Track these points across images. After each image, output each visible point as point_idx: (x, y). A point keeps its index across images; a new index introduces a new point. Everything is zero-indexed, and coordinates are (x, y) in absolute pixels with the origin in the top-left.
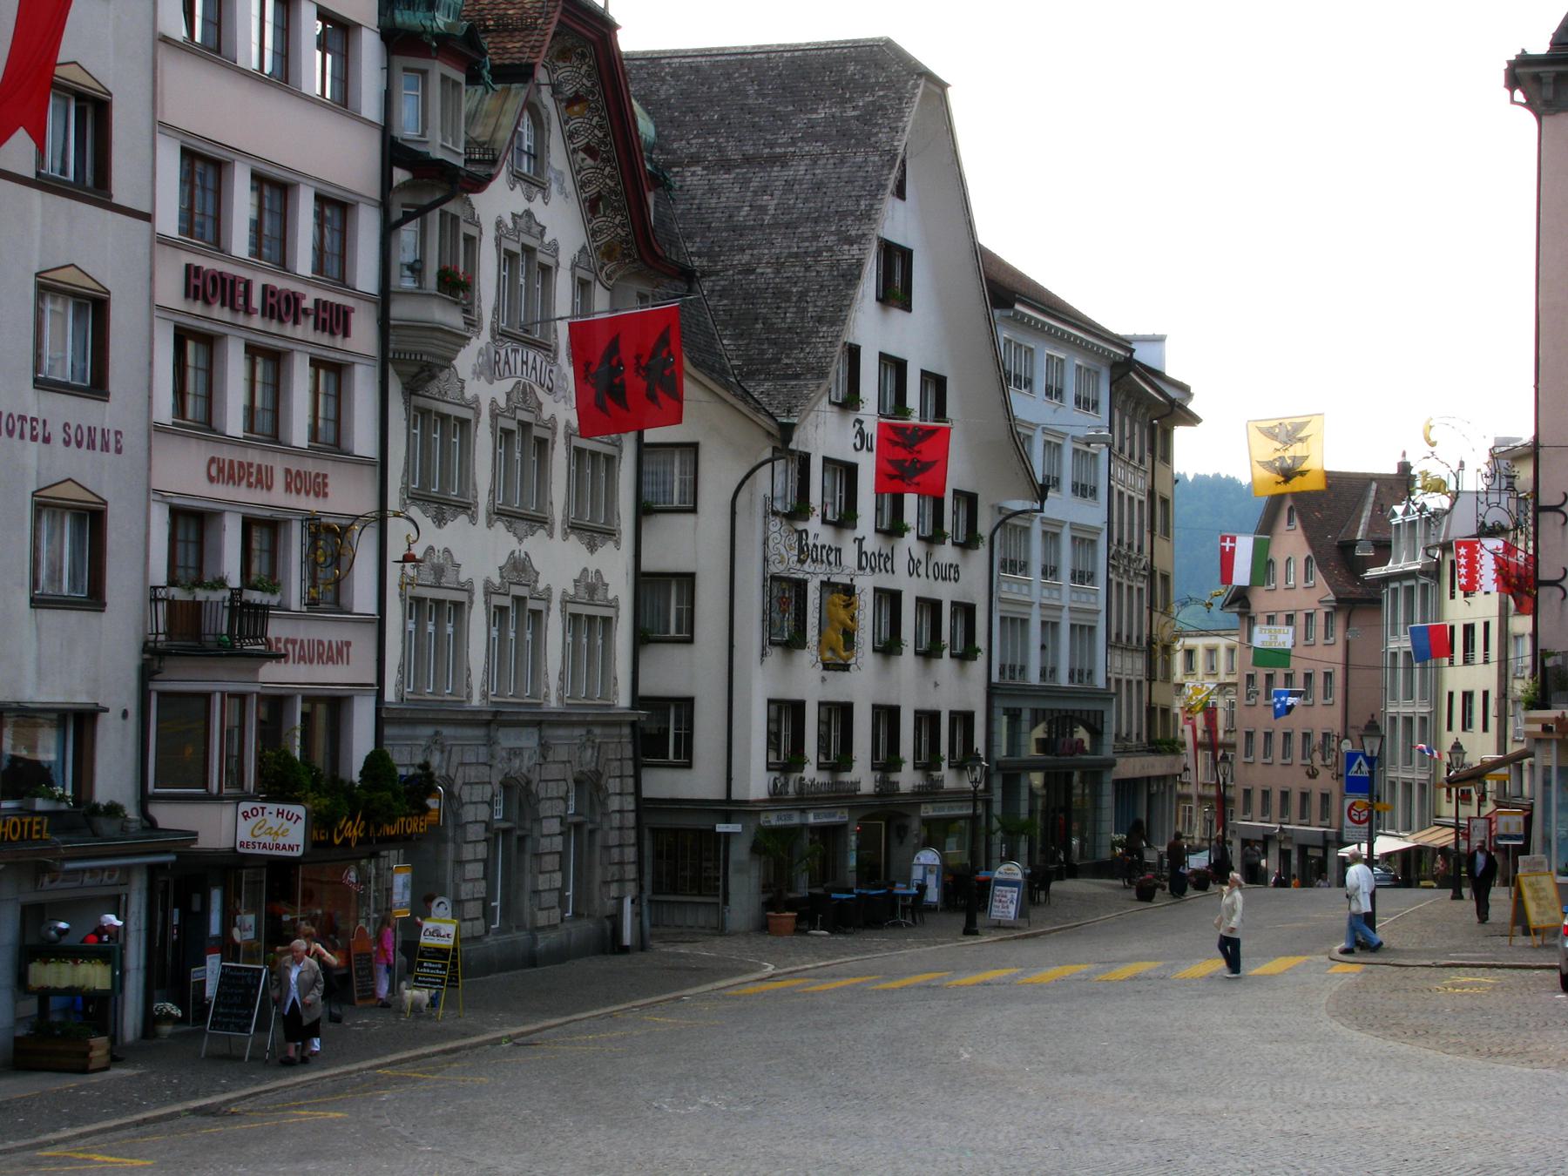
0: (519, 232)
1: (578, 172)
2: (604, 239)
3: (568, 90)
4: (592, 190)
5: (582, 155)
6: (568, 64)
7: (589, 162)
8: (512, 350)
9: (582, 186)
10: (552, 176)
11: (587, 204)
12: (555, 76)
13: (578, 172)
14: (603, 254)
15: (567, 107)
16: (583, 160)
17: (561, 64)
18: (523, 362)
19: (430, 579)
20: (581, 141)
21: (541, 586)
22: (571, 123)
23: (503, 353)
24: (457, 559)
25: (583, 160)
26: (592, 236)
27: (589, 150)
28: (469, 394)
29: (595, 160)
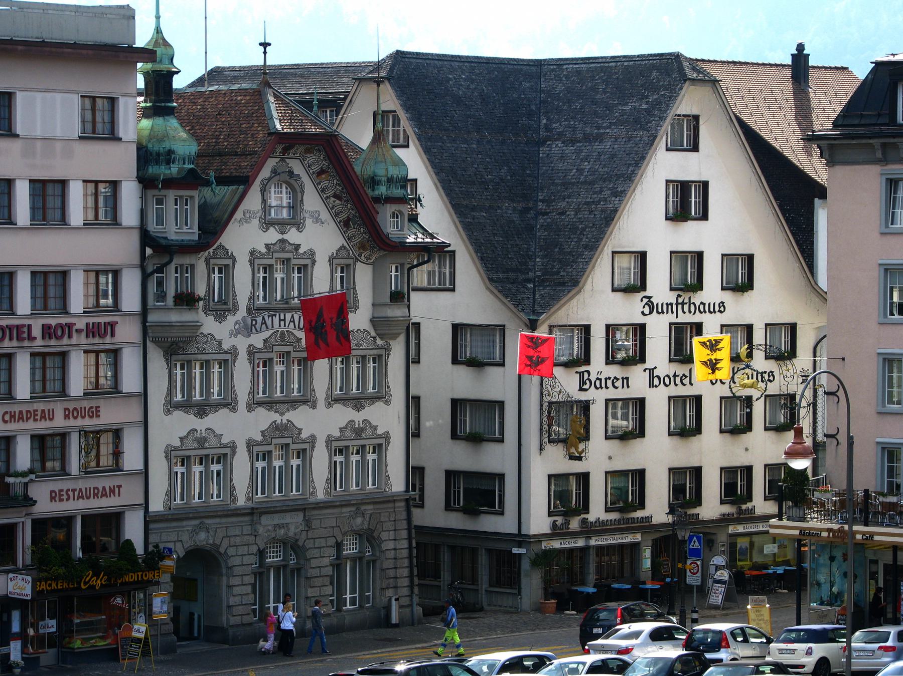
0: (272, 252)
1: (332, 208)
2: (357, 240)
3: (316, 168)
4: (344, 216)
5: (333, 199)
7: (338, 202)
8: (269, 316)
10: (307, 215)
12: (306, 162)
13: (332, 208)
14: (359, 248)
15: (317, 177)
16: (334, 202)
17: (308, 155)
18: (280, 320)
19: (195, 445)
20: (330, 193)
21: (304, 435)
23: (259, 320)
24: (218, 432)
25: (334, 202)
26: (349, 239)
27: (335, 196)
28: (225, 346)
29: (341, 201)
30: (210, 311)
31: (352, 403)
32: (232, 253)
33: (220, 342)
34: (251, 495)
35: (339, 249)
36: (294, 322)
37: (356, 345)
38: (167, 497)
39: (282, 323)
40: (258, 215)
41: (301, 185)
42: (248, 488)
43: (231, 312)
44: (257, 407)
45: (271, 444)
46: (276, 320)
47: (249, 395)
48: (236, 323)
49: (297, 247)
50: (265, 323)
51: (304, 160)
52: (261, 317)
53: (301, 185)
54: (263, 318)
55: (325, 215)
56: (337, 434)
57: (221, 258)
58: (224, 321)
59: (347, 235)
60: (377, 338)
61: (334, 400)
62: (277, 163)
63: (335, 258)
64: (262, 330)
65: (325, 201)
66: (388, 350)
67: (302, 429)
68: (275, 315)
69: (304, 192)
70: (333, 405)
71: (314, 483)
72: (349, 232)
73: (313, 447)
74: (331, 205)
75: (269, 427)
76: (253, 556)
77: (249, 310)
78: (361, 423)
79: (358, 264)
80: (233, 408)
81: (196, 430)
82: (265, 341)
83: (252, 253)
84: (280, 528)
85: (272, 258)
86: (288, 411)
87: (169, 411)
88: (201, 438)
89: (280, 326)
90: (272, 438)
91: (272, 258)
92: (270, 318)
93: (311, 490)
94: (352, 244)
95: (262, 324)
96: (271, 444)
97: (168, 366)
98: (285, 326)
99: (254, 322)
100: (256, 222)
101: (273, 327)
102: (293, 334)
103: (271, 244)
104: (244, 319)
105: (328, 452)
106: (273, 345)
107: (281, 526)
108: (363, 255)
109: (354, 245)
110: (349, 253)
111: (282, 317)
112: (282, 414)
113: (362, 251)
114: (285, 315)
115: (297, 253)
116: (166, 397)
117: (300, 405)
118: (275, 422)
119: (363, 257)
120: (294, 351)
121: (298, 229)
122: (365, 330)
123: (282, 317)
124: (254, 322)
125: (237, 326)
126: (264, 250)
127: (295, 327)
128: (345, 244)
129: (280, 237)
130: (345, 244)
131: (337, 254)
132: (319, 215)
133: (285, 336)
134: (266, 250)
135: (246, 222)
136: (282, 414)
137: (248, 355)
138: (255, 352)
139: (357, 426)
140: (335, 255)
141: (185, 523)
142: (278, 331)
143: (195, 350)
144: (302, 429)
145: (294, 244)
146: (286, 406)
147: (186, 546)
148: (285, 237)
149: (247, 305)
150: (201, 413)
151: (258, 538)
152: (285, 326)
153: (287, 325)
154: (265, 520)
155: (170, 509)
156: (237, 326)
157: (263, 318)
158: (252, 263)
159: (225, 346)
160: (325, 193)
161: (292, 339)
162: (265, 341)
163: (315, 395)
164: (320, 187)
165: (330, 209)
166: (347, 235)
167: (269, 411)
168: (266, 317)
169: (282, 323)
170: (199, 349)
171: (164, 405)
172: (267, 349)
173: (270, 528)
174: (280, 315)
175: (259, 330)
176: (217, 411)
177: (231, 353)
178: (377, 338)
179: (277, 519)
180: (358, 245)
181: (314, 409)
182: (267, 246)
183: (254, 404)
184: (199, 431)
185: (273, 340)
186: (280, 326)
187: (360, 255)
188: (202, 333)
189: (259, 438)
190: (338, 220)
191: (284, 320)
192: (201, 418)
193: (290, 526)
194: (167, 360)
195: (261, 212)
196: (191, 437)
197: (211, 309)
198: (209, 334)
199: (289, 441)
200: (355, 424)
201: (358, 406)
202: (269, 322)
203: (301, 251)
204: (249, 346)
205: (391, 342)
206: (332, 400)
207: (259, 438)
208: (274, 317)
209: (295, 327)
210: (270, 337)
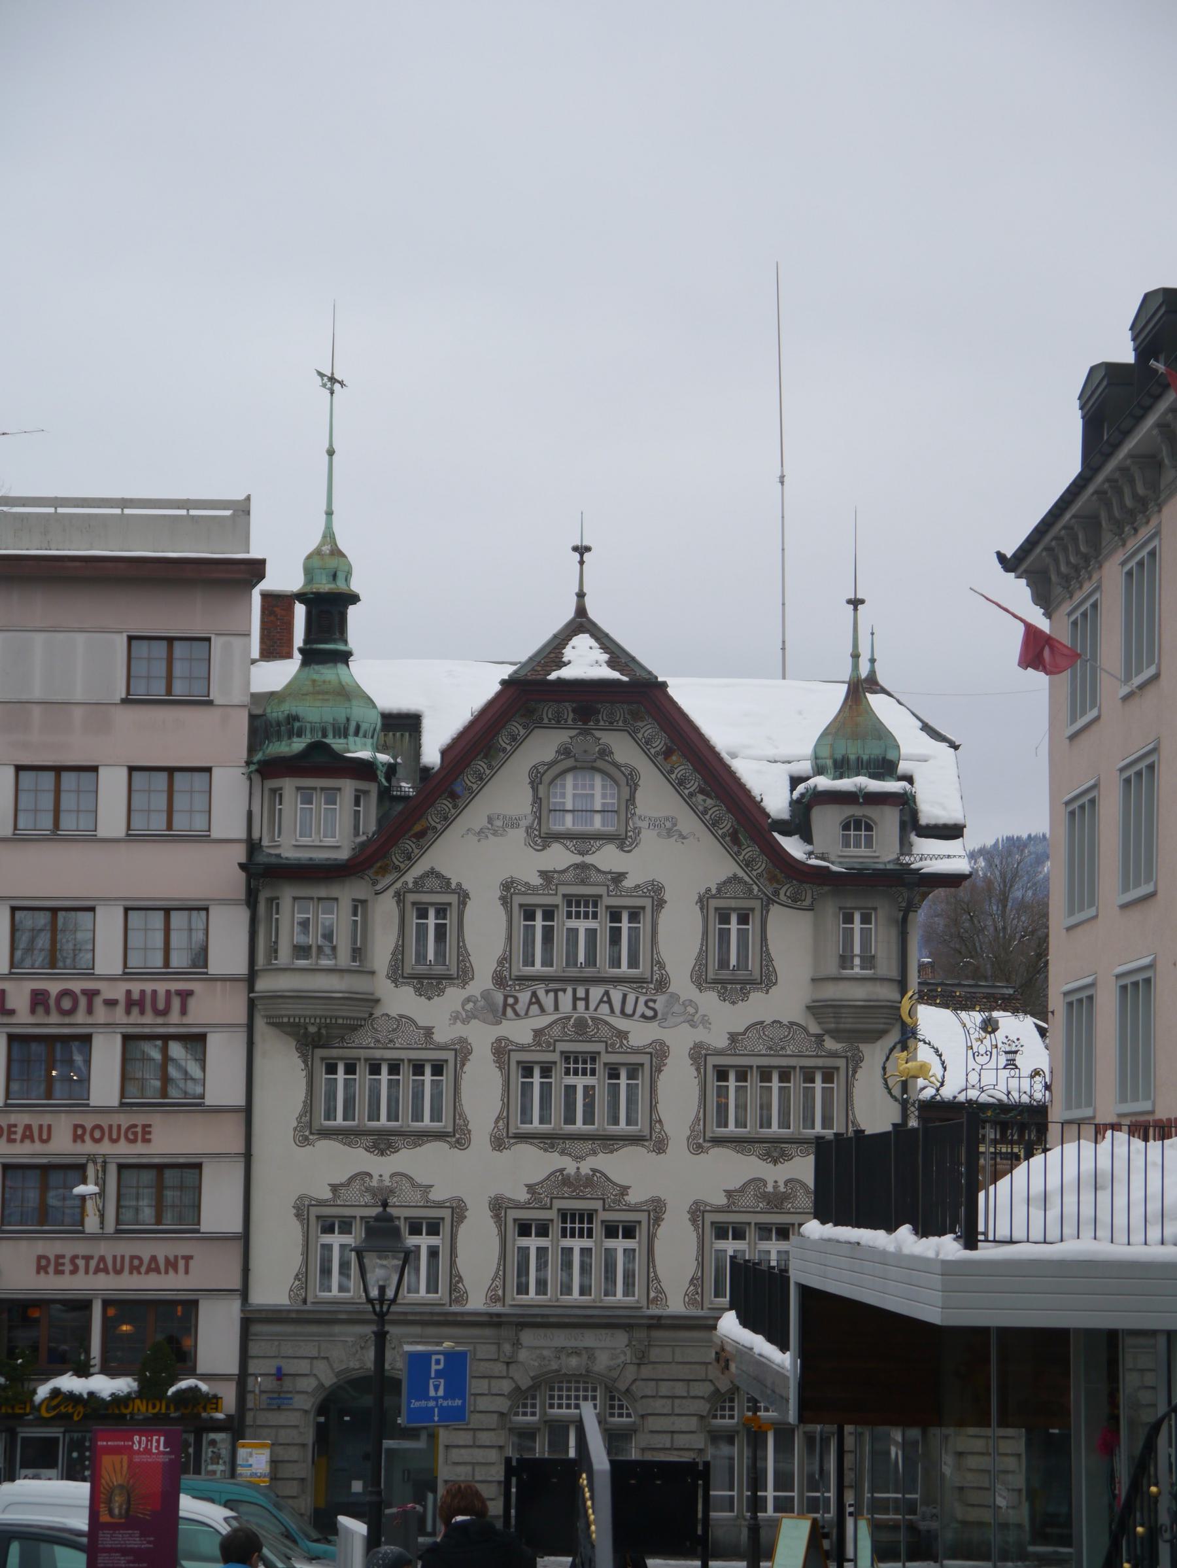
1: (705, 812)
5: (700, 797)
6: (645, 723)
8: (547, 992)
9: (713, 826)
10: (644, 824)
11: (728, 839)
12: (640, 735)
13: (705, 812)
15: (665, 759)
17: (640, 724)
18: (575, 999)
20: (693, 786)
21: (633, 1198)
22: (676, 771)
23: (524, 997)
24: (421, 1179)
25: (704, 801)
26: (747, 865)
28: (440, 1037)
30: (404, 978)
31: (760, 1148)
32: (459, 885)
33: (429, 1031)
34: (500, 1293)
35: (725, 883)
36: (609, 1002)
37: (771, 1049)
38: (297, 1283)
39: (581, 1005)
40: (524, 823)
41: (631, 774)
42: (493, 1280)
43: (456, 981)
44: (516, 1143)
45: (551, 1208)
46: (566, 999)
47: (497, 1122)
48: (468, 1000)
49: (618, 878)
50: (538, 1002)
51: (634, 732)
52: (529, 994)
53: (631, 774)
54: (534, 994)
55: (688, 822)
56: (722, 1200)
57: (432, 892)
58: (438, 995)
59: (741, 857)
60: (826, 1037)
61: (709, 1141)
62: (571, 738)
63: (713, 897)
64: (531, 1013)
65: (688, 800)
66: (855, 1062)
67: (629, 1187)
68: (564, 991)
69: (636, 785)
70: (709, 1148)
71: (659, 1282)
72: (744, 853)
73: (658, 1220)
74: (701, 808)
75: (547, 1178)
76: (502, 1398)
77: (499, 980)
78: (781, 1184)
79: (775, 910)
80: (458, 1141)
81: (370, 1175)
82: (538, 1033)
83: (509, 887)
84: (569, 1355)
85: (556, 894)
86: (595, 1153)
87: (306, 1139)
88: (380, 1189)
89: (575, 1007)
90: (552, 1199)
91: (556, 894)
92: (552, 995)
93: (652, 1295)
94: (755, 873)
95: (531, 1003)
96: (551, 1208)
97: (307, 1065)
98: (587, 1008)
99: (511, 1001)
100: (519, 834)
101: (556, 1008)
102: (606, 1023)
103: (555, 872)
104: (486, 995)
105: (696, 1229)
106: (556, 1041)
107: (576, 1352)
108: (782, 892)
109: (760, 875)
110: (751, 891)
111: (581, 993)
112: (579, 1158)
113: (775, 885)
114: (587, 992)
115: (617, 886)
116: (301, 1116)
117: (626, 1146)
118: (561, 1170)
119: (782, 896)
120: (607, 1052)
121: (621, 847)
122: (792, 1023)
123: (581, 993)
124: (511, 1001)
125: (469, 1006)
126: (536, 881)
127: (612, 1011)
128: (741, 874)
129: (578, 859)
130: (741, 874)
131: (719, 890)
132: (675, 825)
133: (587, 1026)
134: (541, 881)
135: (493, 834)
136: (579, 1158)
137: (494, 1054)
138: (511, 1050)
139: (770, 1189)
140: (714, 891)
141: (337, 1329)
142: (569, 1018)
143: (369, 1041)
144: (629, 1187)
145: (610, 873)
146: (589, 1145)
147: (339, 1367)
148: (588, 859)
149: (495, 971)
150: (382, 1146)
151: (513, 1367)
152: (587, 1008)
153: (592, 1006)
154: (528, 1337)
155: (305, 1301)
156: (469, 1006)
157: (534, 994)
158: (505, 901)
159: (440, 1037)
160: (685, 788)
161: (604, 1031)
162: (538, 1033)
163: (662, 1129)
164: (673, 776)
165: (701, 814)
166: (741, 857)
167: (546, 1150)
168: (541, 994)
169: (581, 1005)
170: (378, 1041)
171: (295, 1129)
172: (540, 1045)
173: (546, 1353)
174: (575, 991)
175: (522, 1013)
176: (420, 1145)
177: (455, 1050)
178: (826, 1037)
179: (561, 1339)
180: (765, 875)
181: (660, 1153)
182: (544, 874)
183: (508, 1137)
184: (376, 1177)
185: (556, 1031)
186: (575, 1007)
187: (776, 893)
188: (387, 1015)
189: (523, 1196)
190: (720, 832)
191: (586, 999)
192: (382, 1155)
193: (597, 1353)
194: (304, 1057)
195: (530, 818)
196: (356, 1185)
197: (405, 975)
198: (401, 1016)
199: (597, 1205)
200: (765, 1186)
201: (775, 1154)
202: (548, 1001)
203: (628, 883)
204: (499, 1040)
205: (862, 1047)
206: (705, 1141)
207: (523, 1196)
208: (560, 994)
209: (612, 1011)
210: (550, 1025)
